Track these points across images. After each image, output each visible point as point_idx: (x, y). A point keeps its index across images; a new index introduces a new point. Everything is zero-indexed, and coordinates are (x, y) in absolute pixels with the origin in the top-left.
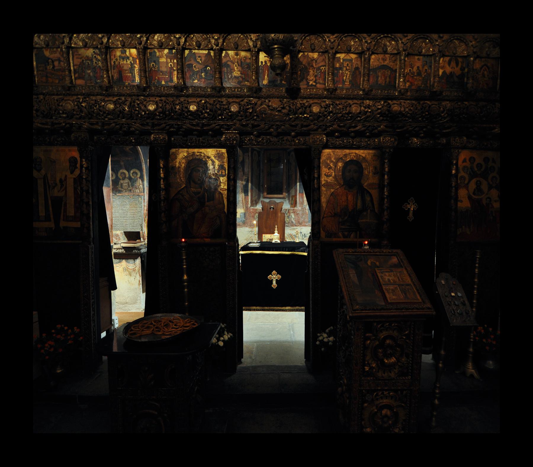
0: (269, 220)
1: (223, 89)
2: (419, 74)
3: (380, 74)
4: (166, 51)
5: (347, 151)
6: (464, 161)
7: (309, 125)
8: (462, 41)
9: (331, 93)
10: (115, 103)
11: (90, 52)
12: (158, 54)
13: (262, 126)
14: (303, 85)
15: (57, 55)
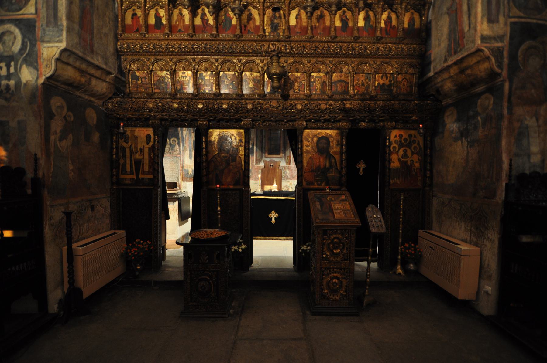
0: (269, 175)
1: (243, 95)
2: (363, 85)
3: (338, 85)
4: (209, 73)
5: (320, 131)
6: (396, 136)
7: (295, 116)
8: (389, 65)
9: (309, 97)
10: (178, 103)
11: (164, 73)
12: (204, 74)
13: (266, 116)
14: (291, 92)
15: (144, 75)
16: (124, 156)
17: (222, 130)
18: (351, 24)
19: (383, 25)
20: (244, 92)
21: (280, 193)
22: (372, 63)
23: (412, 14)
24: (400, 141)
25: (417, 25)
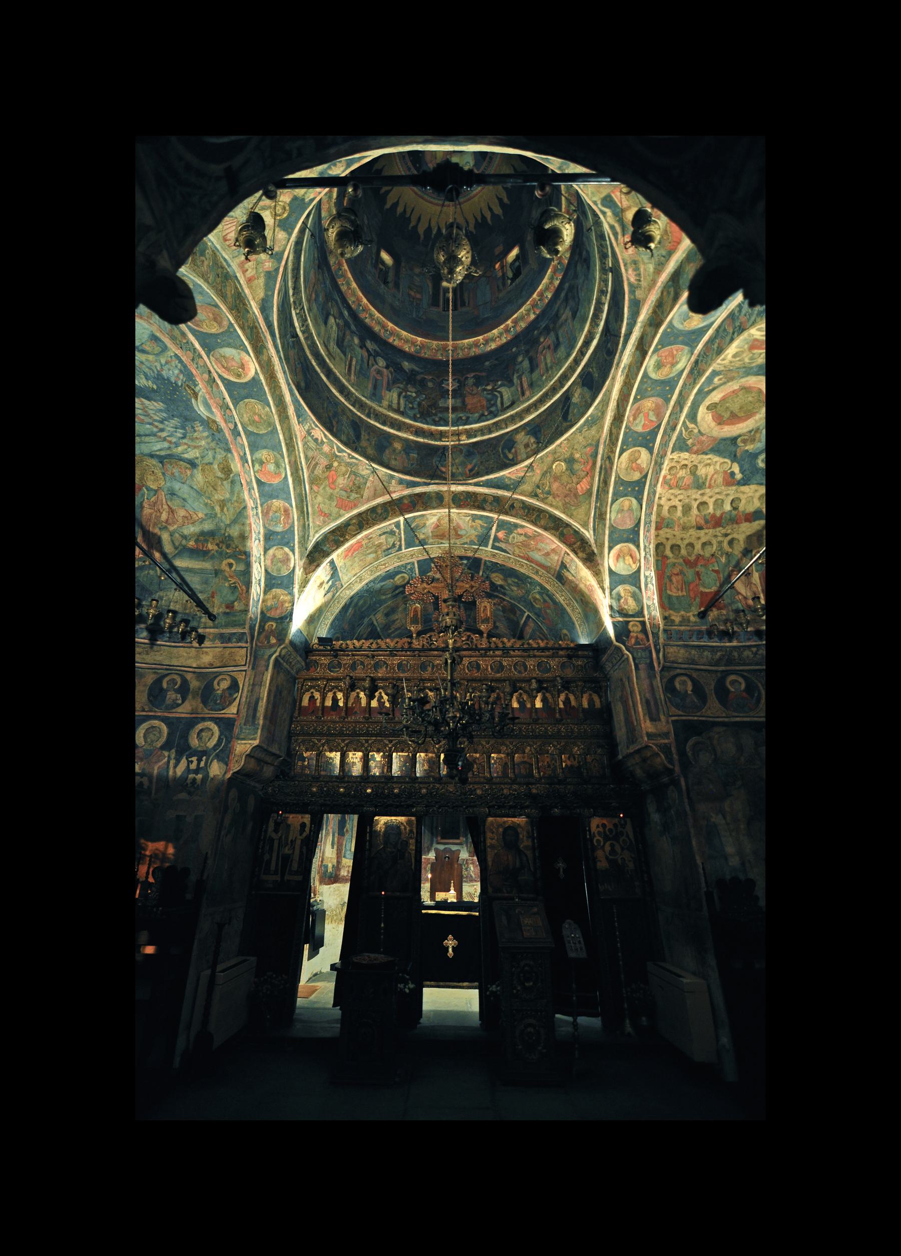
1: (417, 778)
2: (549, 766)
5: (506, 819)
6: (598, 826)
10: (344, 788)
11: (332, 755)
14: (470, 775)
16: (271, 850)
17: (389, 818)
18: (529, 706)
19: (561, 706)
20: (418, 775)
21: (460, 905)
22: (555, 743)
23: (590, 695)
24: (605, 832)
25: (598, 704)
